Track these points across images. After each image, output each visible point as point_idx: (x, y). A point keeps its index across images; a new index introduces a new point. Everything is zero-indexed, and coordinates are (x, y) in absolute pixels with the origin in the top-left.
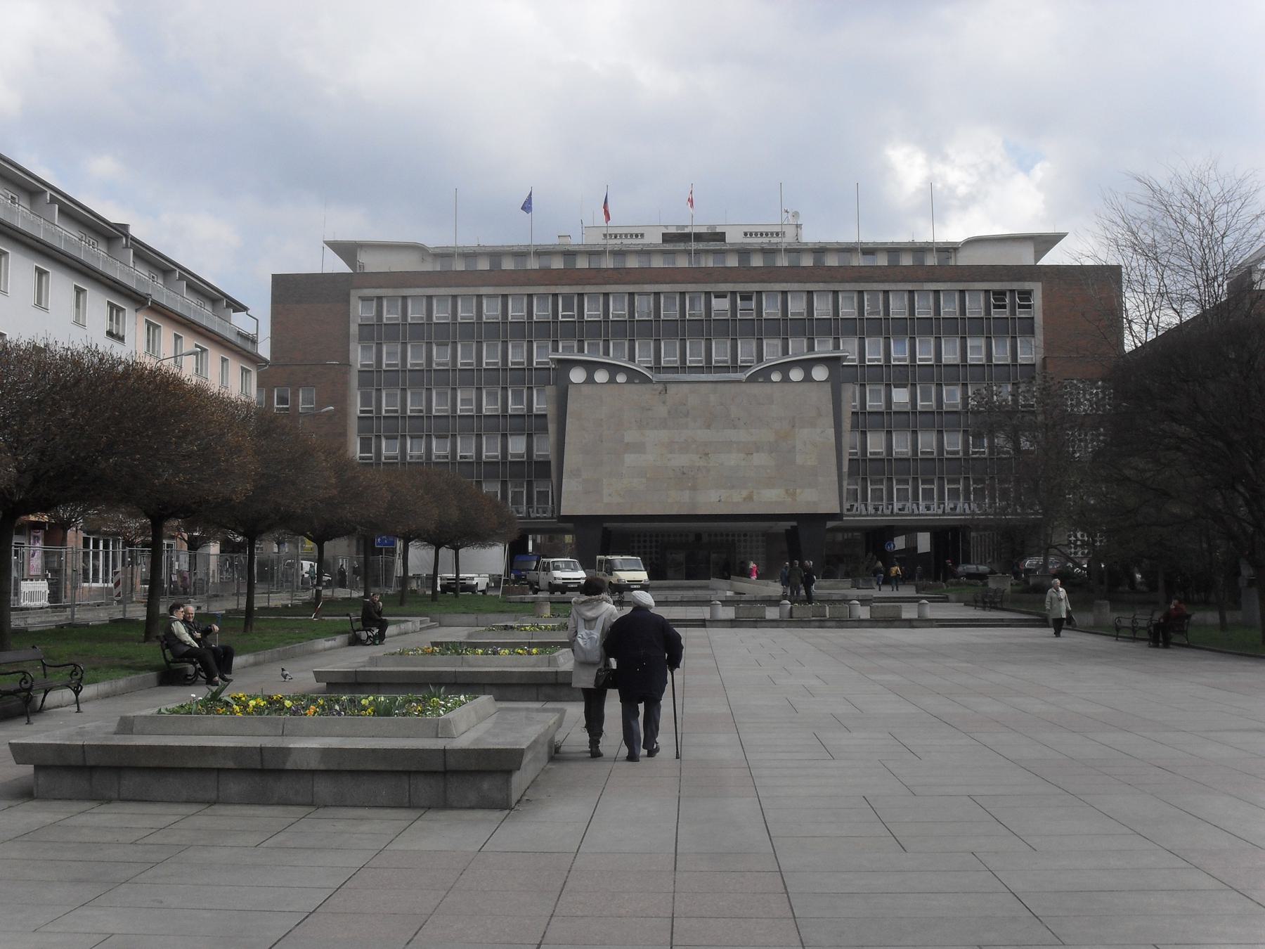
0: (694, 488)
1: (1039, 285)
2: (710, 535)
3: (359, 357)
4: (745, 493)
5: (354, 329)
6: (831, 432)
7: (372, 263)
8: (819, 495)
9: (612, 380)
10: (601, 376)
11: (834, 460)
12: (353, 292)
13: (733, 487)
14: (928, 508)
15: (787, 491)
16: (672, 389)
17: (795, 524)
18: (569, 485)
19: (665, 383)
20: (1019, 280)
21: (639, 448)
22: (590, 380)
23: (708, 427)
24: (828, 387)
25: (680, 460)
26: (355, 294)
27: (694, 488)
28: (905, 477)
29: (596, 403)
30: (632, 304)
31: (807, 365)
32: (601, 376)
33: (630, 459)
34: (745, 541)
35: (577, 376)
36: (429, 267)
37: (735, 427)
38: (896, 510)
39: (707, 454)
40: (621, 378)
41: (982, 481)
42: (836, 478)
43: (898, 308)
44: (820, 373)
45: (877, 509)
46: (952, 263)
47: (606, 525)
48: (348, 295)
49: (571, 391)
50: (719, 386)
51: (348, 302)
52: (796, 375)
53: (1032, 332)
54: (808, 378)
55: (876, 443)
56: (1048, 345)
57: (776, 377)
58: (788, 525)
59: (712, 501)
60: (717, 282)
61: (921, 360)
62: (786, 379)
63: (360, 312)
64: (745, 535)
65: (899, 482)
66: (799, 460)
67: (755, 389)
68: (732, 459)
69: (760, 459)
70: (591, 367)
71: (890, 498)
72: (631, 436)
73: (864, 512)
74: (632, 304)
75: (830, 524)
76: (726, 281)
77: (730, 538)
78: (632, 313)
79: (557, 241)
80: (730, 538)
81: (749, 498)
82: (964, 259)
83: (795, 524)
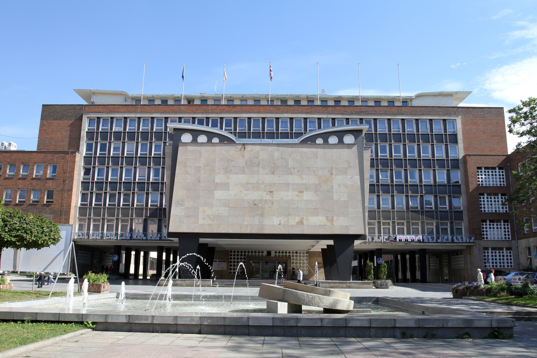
0: (262, 215)
2: (276, 252)
4: (297, 219)
6: (357, 178)
7: (98, 100)
10: (202, 139)
16: (249, 148)
17: (331, 242)
18: (176, 212)
19: (244, 144)
21: (225, 186)
23: (273, 173)
24: (355, 148)
25: (254, 195)
31: (340, 134)
32: (202, 139)
33: (219, 194)
34: (297, 256)
35: (186, 138)
39: (271, 192)
42: (361, 210)
44: (349, 139)
45: (373, 239)
47: (202, 240)
49: (181, 149)
52: (333, 140)
58: (324, 244)
59: (273, 224)
64: (296, 253)
66: (335, 197)
69: (308, 196)
70: (196, 133)
71: (379, 232)
72: (219, 178)
77: (288, 254)
80: (288, 254)
81: (301, 222)
82: (415, 103)
83: (331, 242)
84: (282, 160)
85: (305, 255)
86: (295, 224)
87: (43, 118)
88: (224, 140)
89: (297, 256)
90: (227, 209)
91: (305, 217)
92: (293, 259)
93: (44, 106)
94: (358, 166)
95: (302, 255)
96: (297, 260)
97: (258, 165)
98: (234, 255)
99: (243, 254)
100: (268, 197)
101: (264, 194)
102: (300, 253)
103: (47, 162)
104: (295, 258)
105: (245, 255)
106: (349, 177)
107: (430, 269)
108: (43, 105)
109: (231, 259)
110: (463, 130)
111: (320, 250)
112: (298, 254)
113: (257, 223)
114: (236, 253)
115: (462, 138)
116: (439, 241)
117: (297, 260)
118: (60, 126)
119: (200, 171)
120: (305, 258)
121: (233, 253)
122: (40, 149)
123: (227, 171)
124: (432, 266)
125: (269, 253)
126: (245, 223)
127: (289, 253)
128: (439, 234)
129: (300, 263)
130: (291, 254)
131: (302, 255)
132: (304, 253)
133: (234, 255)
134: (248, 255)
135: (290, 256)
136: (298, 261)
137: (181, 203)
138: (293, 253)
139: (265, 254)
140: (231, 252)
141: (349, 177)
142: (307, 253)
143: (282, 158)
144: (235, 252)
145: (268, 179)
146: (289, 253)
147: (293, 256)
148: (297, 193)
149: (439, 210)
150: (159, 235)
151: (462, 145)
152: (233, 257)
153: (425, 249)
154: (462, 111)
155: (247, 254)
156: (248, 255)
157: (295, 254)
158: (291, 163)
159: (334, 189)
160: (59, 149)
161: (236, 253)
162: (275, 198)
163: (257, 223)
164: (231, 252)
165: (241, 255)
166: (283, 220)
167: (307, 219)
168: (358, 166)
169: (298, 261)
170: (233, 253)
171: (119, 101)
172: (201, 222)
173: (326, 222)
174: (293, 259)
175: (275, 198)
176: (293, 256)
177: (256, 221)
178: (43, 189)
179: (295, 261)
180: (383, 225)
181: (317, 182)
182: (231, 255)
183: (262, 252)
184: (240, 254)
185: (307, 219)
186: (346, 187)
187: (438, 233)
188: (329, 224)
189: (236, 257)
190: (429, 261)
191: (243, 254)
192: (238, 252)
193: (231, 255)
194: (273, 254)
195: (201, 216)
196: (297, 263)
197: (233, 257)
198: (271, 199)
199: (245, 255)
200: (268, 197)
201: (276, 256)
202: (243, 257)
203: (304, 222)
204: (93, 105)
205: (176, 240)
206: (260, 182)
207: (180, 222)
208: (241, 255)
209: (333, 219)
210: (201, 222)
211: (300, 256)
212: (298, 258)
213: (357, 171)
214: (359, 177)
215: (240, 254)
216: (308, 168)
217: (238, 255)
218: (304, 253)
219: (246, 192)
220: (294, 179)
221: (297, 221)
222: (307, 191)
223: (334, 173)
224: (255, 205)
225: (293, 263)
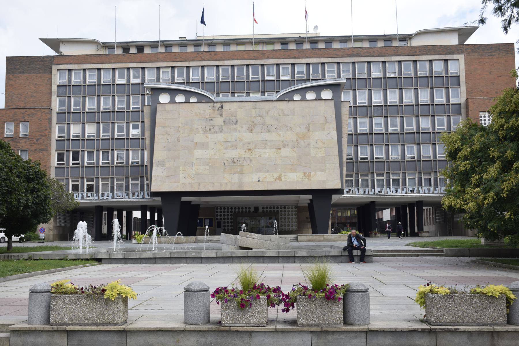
0: (241, 172)
1: (463, 56)
2: (263, 208)
3: (56, 105)
4: (276, 175)
5: (54, 88)
6: (334, 133)
8: (328, 178)
9: (187, 102)
11: (336, 152)
12: (54, 67)
13: (267, 172)
14: (397, 191)
15: (305, 173)
17: (310, 197)
18: (157, 172)
20: (450, 54)
21: (204, 145)
22: (172, 102)
23: (251, 131)
24: (332, 104)
25: (233, 154)
26: (55, 68)
27: (241, 172)
28: (381, 172)
29: (175, 117)
30: (218, 72)
31: (318, 89)
33: (199, 153)
34: (285, 211)
36: (101, 52)
37: (269, 131)
38: (377, 192)
39: (250, 150)
40: (193, 100)
41: (430, 174)
42: (338, 165)
43: (376, 72)
44: (327, 94)
46: (409, 45)
47: (184, 199)
48: (51, 68)
50: (258, 104)
51: (51, 72)
53: (459, 85)
54: (319, 99)
55: (363, 153)
56: (468, 92)
57: (297, 97)
59: (252, 181)
60: (268, 58)
61: (390, 102)
62: (304, 99)
63: (58, 78)
64: (285, 208)
65: (378, 175)
66: (313, 152)
67: (283, 105)
68: (267, 153)
69: (286, 152)
70: (173, 92)
72: (199, 137)
73: (357, 193)
74: (218, 72)
75: (335, 198)
76: (273, 58)
77: (276, 209)
78: (218, 78)
79: (179, 39)
80: (276, 209)
81: (279, 179)
82: (415, 43)
84: (259, 118)
85: (294, 209)
86: (273, 180)
87: (8, 71)
88: (202, 99)
89: (285, 211)
90: (208, 167)
91: (283, 174)
92: (282, 215)
93: (8, 58)
94: (335, 122)
95: (290, 210)
96: (285, 215)
97: (236, 123)
98: (221, 212)
99: (230, 210)
100: (247, 156)
101: (243, 152)
102: (288, 208)
103: (17, 120)
104: (283, 213)
105: (231, 212)
106: (326, 133)
107: (436, 222)
108: (8, 58)
109: (217, 215)
110: (466, 71)
111: (307, 205)
112: (287, 209)
113: (237, 181)
114: (222, 210)
115: (464, 80)
116: (436, 192)
117: (285, 215)
118: (28, 80)
119: (179, 131)
120: (294, 213)
121: (219, 210)
122: (9, 106)
123: (207, 130)
124: (439, 219)
125: (256, 208)
126: (225, 181)
127: (277, 208)
128: (437, 185)
129: (289, 218)
130: (279, 209)
131: (290, 210)
132: (292, 208)
133: (221, 212)
134: (235, 211)
135: (278, 211)
136: (287, 216)
137: (162, 163)
138: (281, 208)
139: (252, 209)
140: (217, 209)
141: (326, 133)
142: (296, 208)
143: (260, 116)
144: (221, 209)
145: (247, 136)
146: (277, 208)
147: (281, 211)
148: (274, 150)
149: (438, 159)
150: (142, 193)
151: (465, 87)
152: (219, 214)
153: (422, 201)
154: (466, 50)
155: (233, 210)
156: (235, 211)
157: (283, 209)
158: (269, 121)
159: (311, 145)
160: (29, 106)
161: (222, 210)
162: (253, 156)
163: (237, 181)
164: (217, 209)
165: (228, 212)
166: (261, 176)
167: (285, 176)
168: (335, 122)
169: (287, 216)
170: (219, 210)
171: (89, 50)
172: (182, 181)
173: (304, 177)
174: (282, 215)
175: (253, 156)
176: (281, 211)
177: (235, 178)
178: (16, 149)
179: (283, 217)
180: (377, 177)
181: (294, 139)
182: (217, 212)
183: (250, 208)
184: (226, 210)
185: (285, 176)
186: (323, 142)
187: (436, 184)
188: (307, 180)
189: (222, 214)
190: (436, 214)
191: (230, 210)
192: (224, 208)
193: (217, 212)
194: (261, 210)
195: (182, 175)
196: (285, 218)
197: (219, 214)
198: (249, 156)
199: (231, 212)
200: (247, 156)
201: (263, 211)
202: (230, 214)
203: (283, 178)
204: (62, 56)
205: (159, 199)
206: (238, 140)
207: (162, 182)
208: (228, 212)
209: (310, 175)
210: (182, 181)
211: (289, 211)
212: (287, 213)
213: (334, 126)
214: (336, 132)
215: (226, 210)
216: (285, 125)
217: (224, 212)
218: (292, 208)
219: (225, 151)
220: (272, 137)
221: (275, 177)
222: (284, 147)
223: (311, 129)
224: (235, 163)
225: (281, 218)
